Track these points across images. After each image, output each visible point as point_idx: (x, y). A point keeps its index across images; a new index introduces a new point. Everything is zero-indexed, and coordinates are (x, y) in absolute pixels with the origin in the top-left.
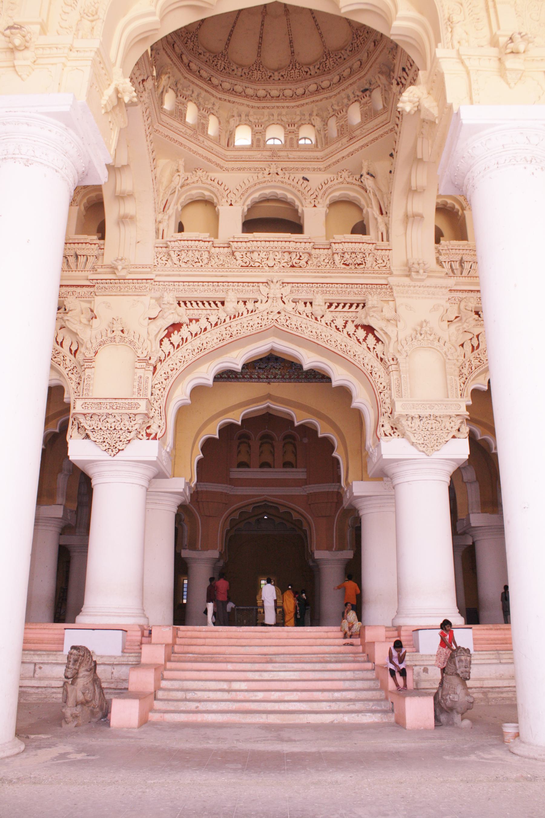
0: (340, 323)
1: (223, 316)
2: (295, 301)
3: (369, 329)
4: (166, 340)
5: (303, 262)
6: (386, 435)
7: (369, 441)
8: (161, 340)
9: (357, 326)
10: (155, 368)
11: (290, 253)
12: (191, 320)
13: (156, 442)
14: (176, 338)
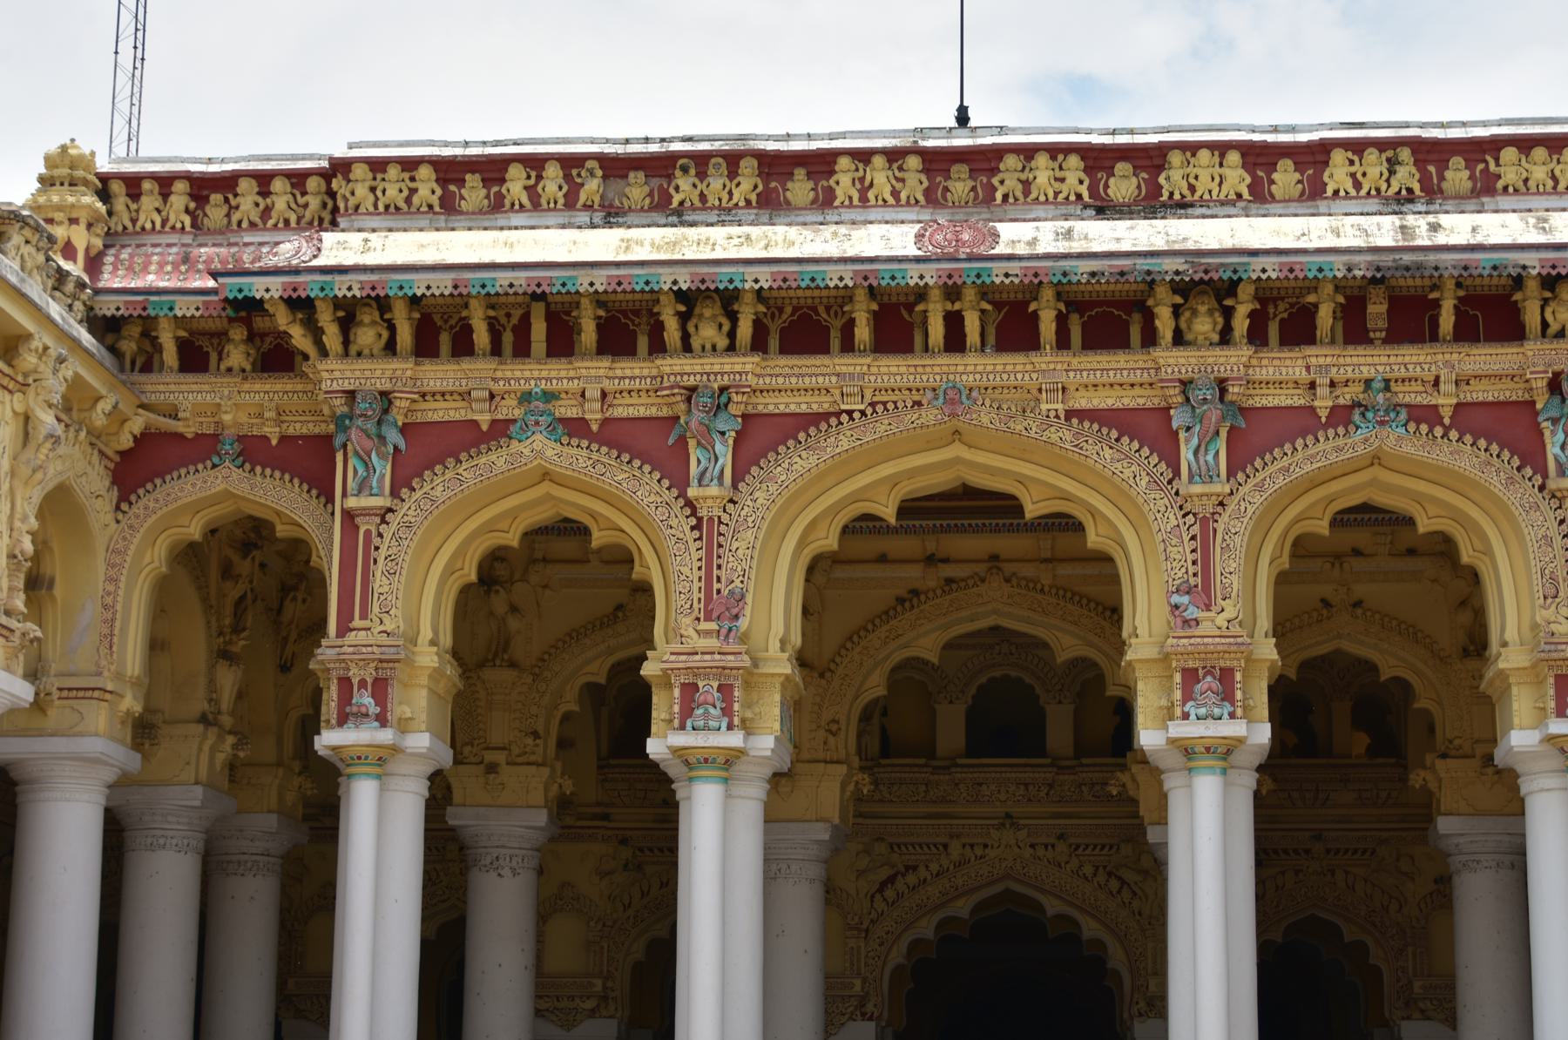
0: (1088, 870)
1: (945, 862)
2: (1032, 846)
3: (1123, 882)
4: (878, 896)
5: (1042, 794)
6: (1141, 1015)
7: (1126, 1015)
8: (873, 896)
9: (1110, 874)
10: (867, 931)
11: (1026, 785)
12: (907, 868)
13: (873, 1024)
14: (890, 893)
